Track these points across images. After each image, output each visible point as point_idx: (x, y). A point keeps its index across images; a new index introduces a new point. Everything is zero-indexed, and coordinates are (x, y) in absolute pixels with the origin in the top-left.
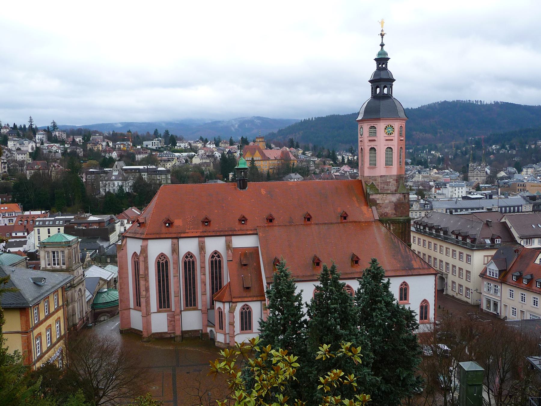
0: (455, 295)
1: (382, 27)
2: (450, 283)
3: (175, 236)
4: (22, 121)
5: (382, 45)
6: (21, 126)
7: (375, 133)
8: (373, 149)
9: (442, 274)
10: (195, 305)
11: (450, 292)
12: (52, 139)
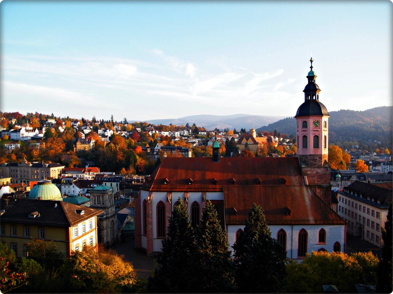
0: (369, 240)
2: (366, 232)
3: (169, 190)
4: (107, 119)
5: (311, 67)
6: (107, 121)
8: (305, 137)
9: (361, 225)
11: (366, 238)
12: (124, 129)
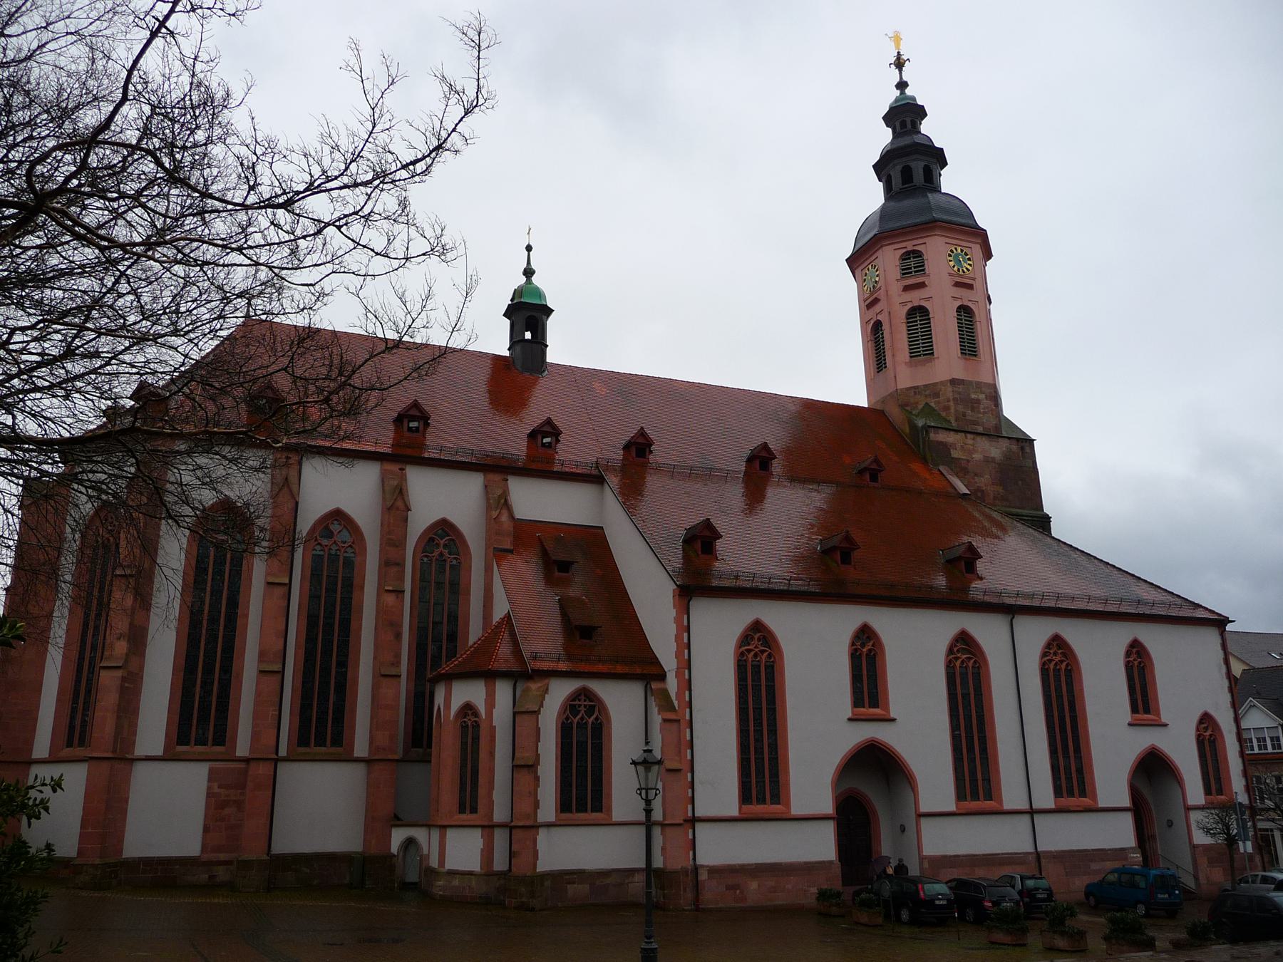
1: (898, 45)
7: (921, 269)
8: (919, 314)
10: (337, 741)
